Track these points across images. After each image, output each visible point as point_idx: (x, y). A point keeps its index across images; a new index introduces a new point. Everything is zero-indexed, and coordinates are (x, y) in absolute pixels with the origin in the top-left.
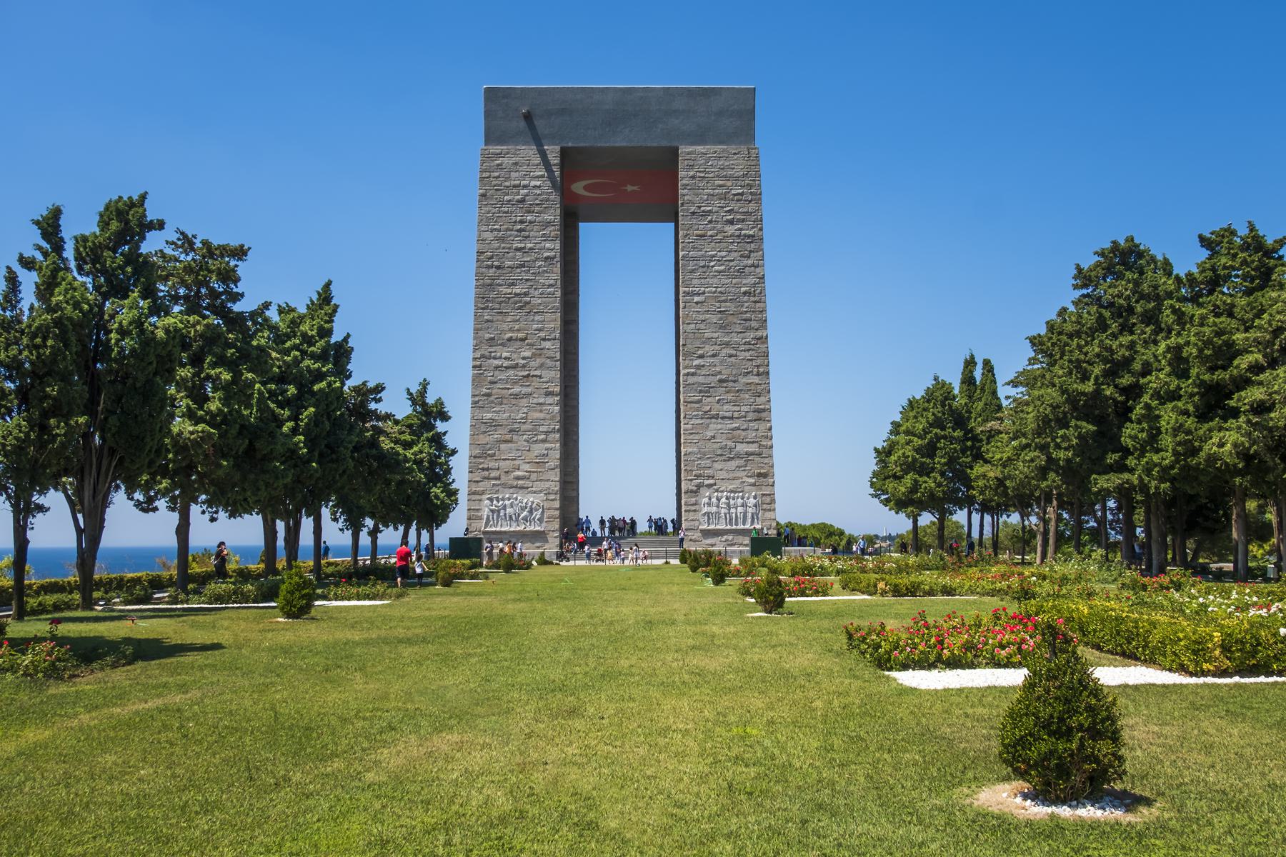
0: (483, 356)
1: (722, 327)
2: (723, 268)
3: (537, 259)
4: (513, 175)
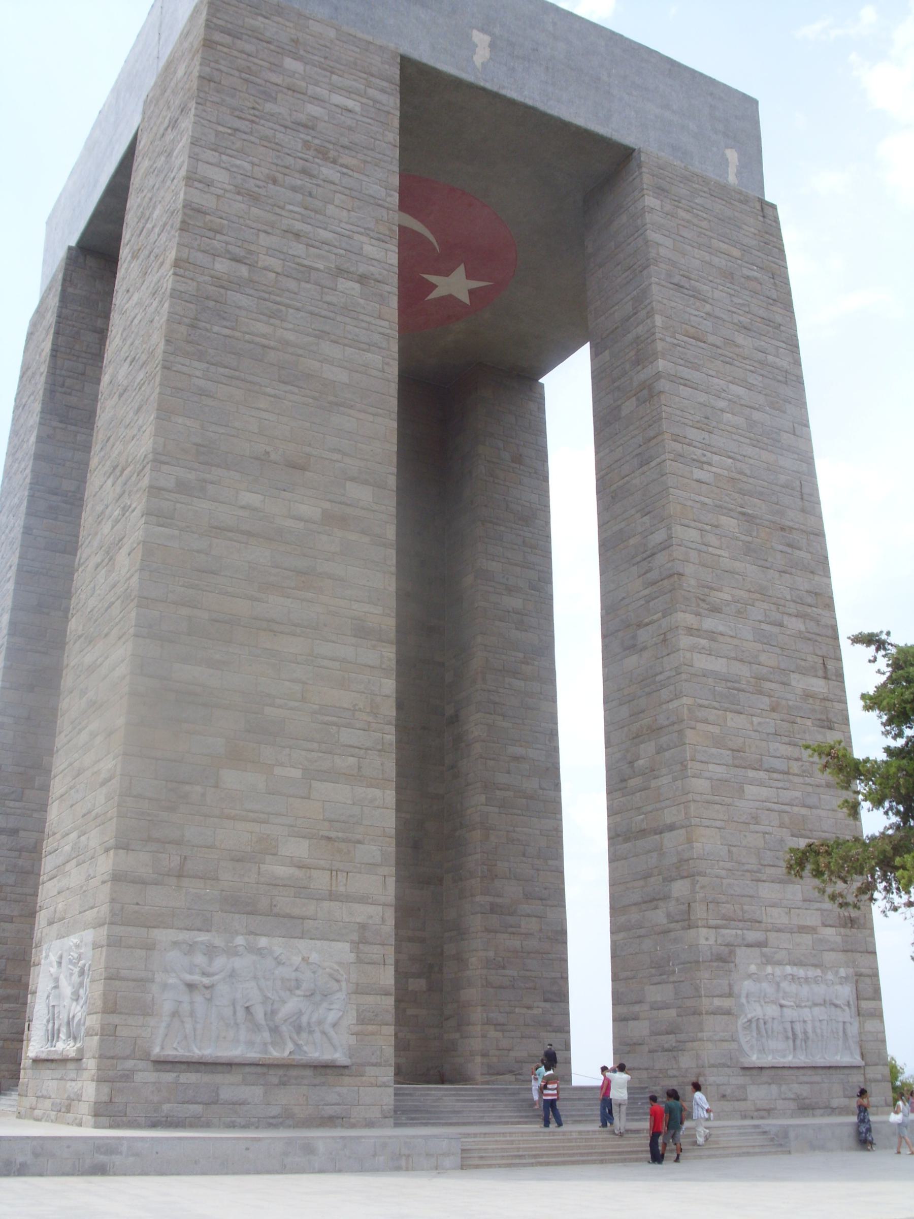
0: (182, 487)
2: (740, 421)
3: (341, 272)
4: (290, 63)
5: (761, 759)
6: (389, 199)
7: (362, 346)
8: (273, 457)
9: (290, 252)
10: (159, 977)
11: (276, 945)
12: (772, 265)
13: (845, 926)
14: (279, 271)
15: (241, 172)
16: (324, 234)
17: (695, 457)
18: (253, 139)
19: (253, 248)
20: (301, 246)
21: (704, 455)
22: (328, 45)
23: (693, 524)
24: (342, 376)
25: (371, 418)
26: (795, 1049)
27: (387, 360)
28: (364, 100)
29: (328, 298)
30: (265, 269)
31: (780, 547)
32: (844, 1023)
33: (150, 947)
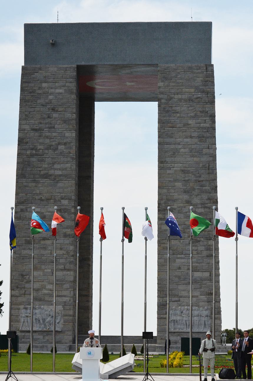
1: (185, 192)
3: (59, 144)
5: (183, 252)
6: (73, 117)
7: (65, 163)
8: (43, 198)
9: (46, 142)
10: (21, 315)
11: (46, 307)
12: (208, 89)
13: (209, 295)
14: (43, 149)
15: (32, 124)
16: (54, 134)
17: (168, 167)
18: (35, 113)
19: (36, 145)
20: (49, 140)
21: (171, 165)
22: (54, 74)
23: (165, 188)
24: (60, 173)
25: (67, 182)
26: (187, 327)
27: (72, 165)
28: (65, 88)
29: (55, 153)
30: (40, 149)
31: (197, 187)
32: (205, 321)
33: (19, 309)
